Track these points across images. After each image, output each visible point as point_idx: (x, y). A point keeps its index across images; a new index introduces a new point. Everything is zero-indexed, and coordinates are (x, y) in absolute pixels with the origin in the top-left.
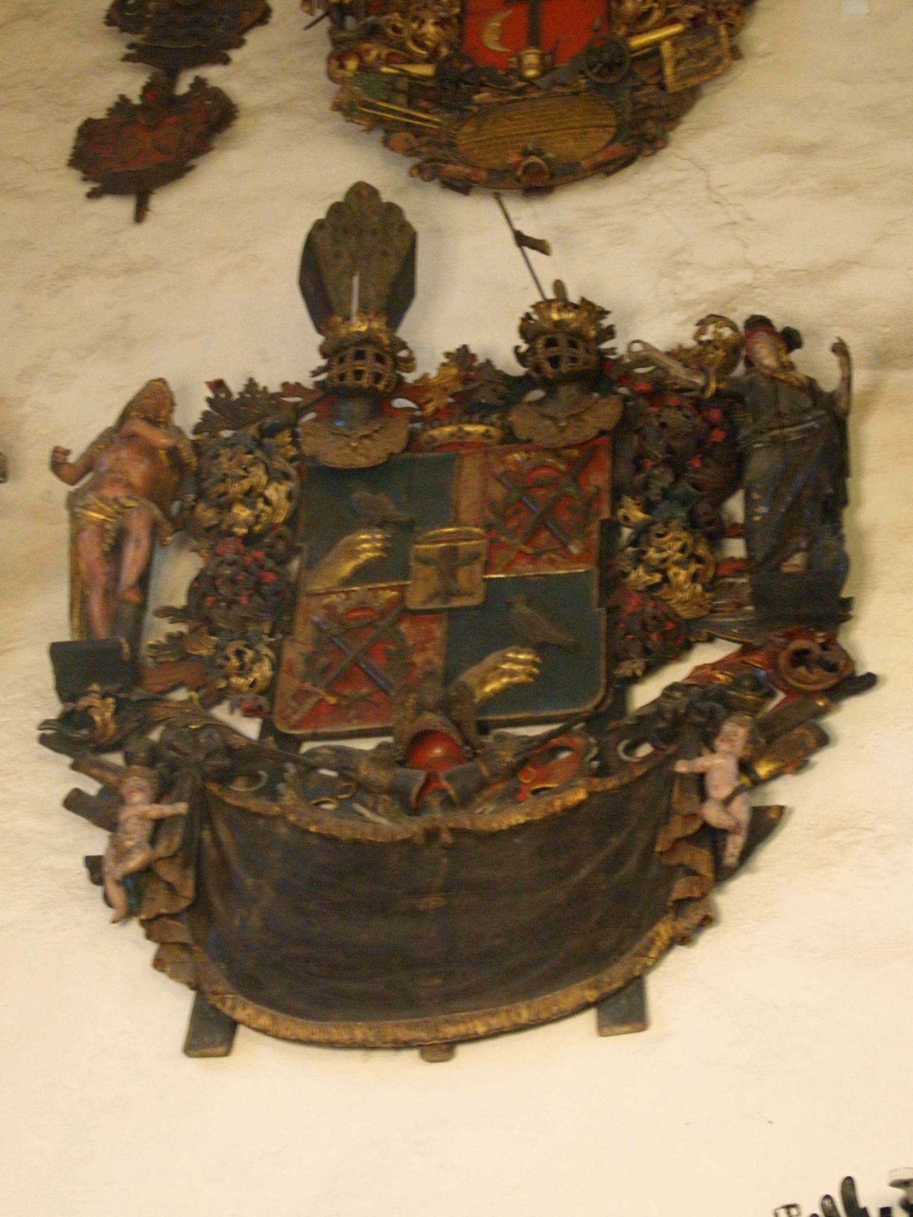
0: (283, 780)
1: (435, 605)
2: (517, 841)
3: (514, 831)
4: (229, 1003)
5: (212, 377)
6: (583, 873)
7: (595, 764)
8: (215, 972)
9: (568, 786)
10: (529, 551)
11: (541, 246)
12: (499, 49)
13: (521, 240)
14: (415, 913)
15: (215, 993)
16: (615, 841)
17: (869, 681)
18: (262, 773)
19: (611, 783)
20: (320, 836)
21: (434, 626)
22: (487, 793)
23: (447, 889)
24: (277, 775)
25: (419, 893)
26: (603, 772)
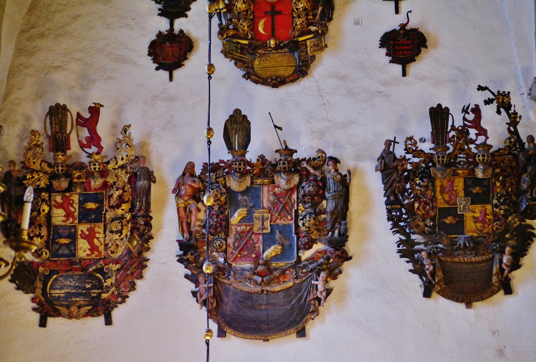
0: (230, 275)
1: (260, 232)
2: (280, 293)
3: (279, 291)
4: (225, 328)
5: (204, 162)
6: (294, 302)
7: (295, 276)
8: (221, 321)
9: (290, 281)
10: (280, 217)
11: (280, 129)
12: (263, 32)
13: (276, 127)
14: (261, 310)
15: (222, 326)
16: (299, 295)
17: (351, 258)
18: (226, 273)
19: (298, 281)
20: (241, 290)
21: (260, 236)
22: (273, 281)
23: (266, 305)
24: (229, 274)
25: (261, 305)
26: (297, 278)
